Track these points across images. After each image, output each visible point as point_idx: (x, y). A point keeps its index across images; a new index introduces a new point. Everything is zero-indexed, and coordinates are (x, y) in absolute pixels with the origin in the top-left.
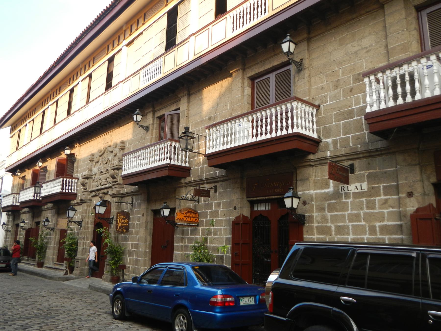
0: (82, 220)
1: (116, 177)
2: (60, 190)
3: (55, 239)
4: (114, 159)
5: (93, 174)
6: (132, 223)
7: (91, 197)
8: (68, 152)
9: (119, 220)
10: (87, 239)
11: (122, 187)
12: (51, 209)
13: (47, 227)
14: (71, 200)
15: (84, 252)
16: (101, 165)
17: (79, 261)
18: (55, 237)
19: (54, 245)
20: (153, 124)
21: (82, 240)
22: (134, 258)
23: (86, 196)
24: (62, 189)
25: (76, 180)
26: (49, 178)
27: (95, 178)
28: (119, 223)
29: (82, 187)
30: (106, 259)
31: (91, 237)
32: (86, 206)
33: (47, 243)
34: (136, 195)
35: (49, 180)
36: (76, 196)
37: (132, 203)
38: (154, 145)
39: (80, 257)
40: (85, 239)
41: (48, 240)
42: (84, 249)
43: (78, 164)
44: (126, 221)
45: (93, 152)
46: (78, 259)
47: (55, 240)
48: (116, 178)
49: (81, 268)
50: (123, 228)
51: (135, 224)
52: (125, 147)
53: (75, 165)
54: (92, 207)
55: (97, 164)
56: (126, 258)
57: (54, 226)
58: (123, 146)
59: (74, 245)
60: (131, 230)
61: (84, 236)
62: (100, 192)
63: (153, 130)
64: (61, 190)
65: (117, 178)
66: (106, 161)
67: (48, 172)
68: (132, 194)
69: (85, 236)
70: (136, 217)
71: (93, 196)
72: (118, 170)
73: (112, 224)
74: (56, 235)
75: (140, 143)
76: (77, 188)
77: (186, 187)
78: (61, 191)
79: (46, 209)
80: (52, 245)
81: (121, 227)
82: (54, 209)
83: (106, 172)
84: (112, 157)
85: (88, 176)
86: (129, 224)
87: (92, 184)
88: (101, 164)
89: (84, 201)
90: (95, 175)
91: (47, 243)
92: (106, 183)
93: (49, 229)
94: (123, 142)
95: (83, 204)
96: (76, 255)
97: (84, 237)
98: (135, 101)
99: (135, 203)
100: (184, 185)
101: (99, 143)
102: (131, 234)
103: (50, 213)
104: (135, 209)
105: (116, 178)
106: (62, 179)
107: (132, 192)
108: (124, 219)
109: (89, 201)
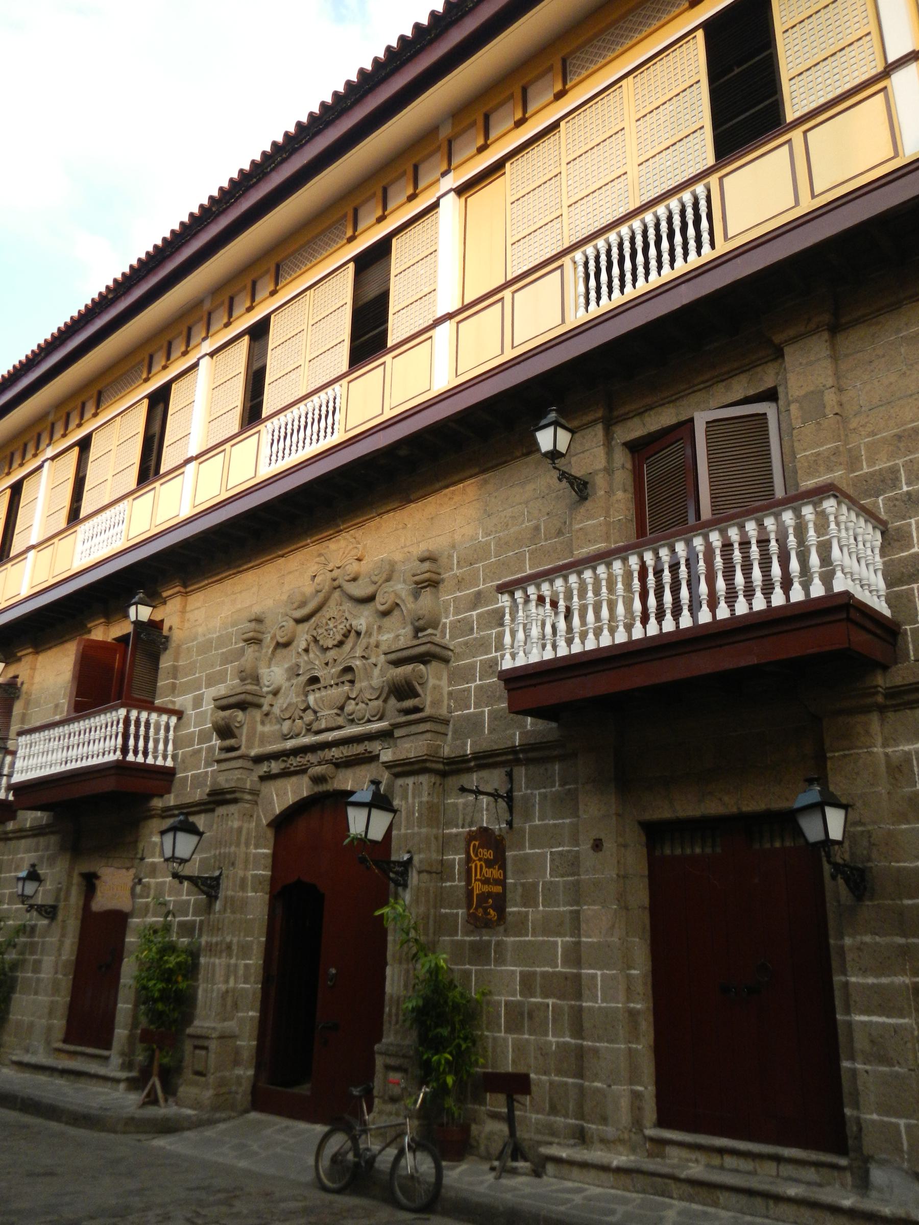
0: (221, 874)
1: (419, 689)
2: (118, 755)
3: (59, 950)
4: (380, 627)
5: (265, 689)
6: (515, 885)
7: (256, 779)
8: (143, 613)
9: (476, 866)
10: (245, 950)
11: (442, 731)
12: (37, 832)
13: (32, 902)
14: (152, 796)
15: (229, 1008)
16: (311, 655)
17: (213, 1045)
18: (61, 943)
19: (56, 973)
20: (609, 471)
21: (224, 954)
22: (550, 1038)
23: (237, 774)
24: (125, 750)
25: (174, 720)
26: (23, 719)
27: (272, 705)
28: (476, 880)
29: (216, 742)
30: (379, 1039)
31: (259, 942)
32: (236, 815)
33: (15, 966)
34: (528, 762)
35: (26, 727)
36: (172, 781)
37: (509, 799)
38: (621, 553)
39: (214, 1029)
40: (235, 952)
41: (22, 953)
42: (230, 994)
43: (176, 659)
44: (496, 873)
45: (257, 610)
46: (207, 1038)
47: (60, 955)
48: (417, 695)
49: (218, 1074)
50: (487, 902)
51: (535, 885)
52: (439, 574)
53: (165, 662)
54: (264, 822)
55: (281, 652)
56: (495, 1039)
57: (57, 899)
58: (434, 573)
59: (180, 979)
60: (514, 913)
61: (228, 939)
62: (311, 758)
63: (610, 493)
64: (118, 753)
65: (423, 695)
66: (339, 637)
67: (23, 696)
68: (510, 757)
69: (235, 940)
70: (544, 854)
71: (267, 778)
72: (425, 663)
73: (405, 886)
74: (63, 935)
75: (532, 553)
76: (175, 748)
77: (882, 709)
78: (121, 758)
79: (10, 835)
80: (46, 974)
81: (483, 897)
82: (52, 833)
83: (341, 679)
84: (371, 619)
85: (249, 698)
86: (502, 883)
87: (260, 728)
88: (306, 650)
89: (229, 796)
90: (275, 693)
91: (15, 966)
92: (340, 721)
93: (36, 910)
94: (429, 558)
95: (221, 810)
96: (188, 1019)
97: (231, 941)
98: (594, 349)
99: (526, 799)
100: (880, 699)
101: (290, 573)
102: (520, 927)
103: (28, 851)
104: (528, 816)
105: (417, 695)
106: (122, 712)
107: (513, 750)
108: (489, 864)
109: (248, 797)
